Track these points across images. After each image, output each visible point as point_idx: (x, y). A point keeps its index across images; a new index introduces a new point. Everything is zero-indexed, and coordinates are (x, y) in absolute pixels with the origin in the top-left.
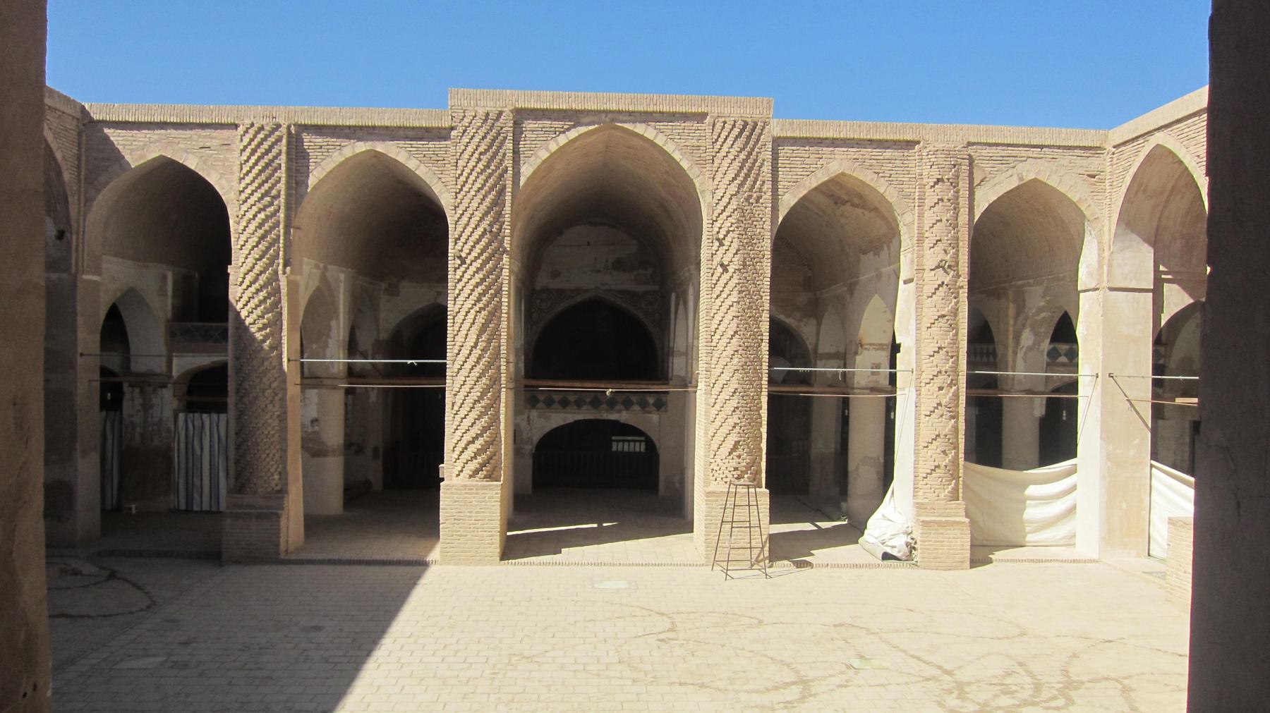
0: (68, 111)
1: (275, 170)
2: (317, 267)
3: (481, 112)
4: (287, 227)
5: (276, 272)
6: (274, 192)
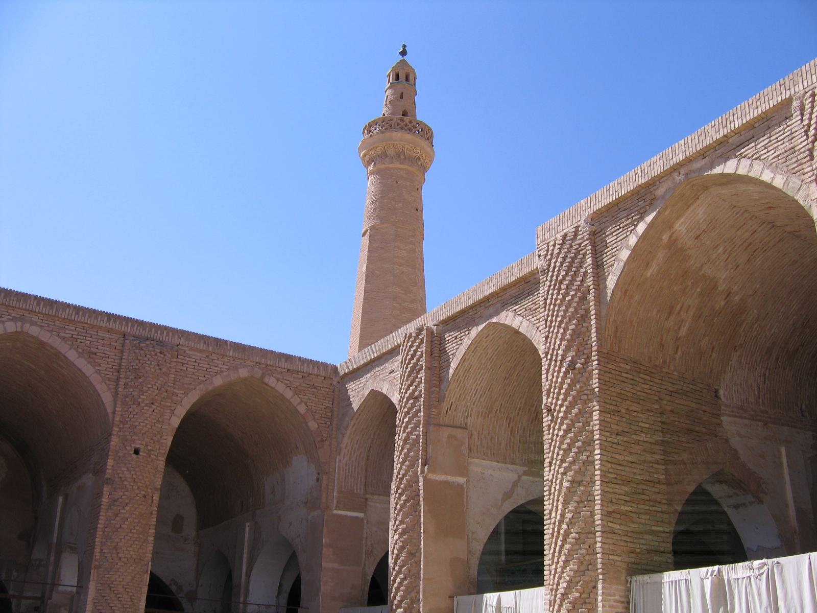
0: (315, 371)
1: (419, 372)
2: (525, 473)
3: (559, 236)
4: (427, 423)
5: (416, 474)
6: (416, 393)
